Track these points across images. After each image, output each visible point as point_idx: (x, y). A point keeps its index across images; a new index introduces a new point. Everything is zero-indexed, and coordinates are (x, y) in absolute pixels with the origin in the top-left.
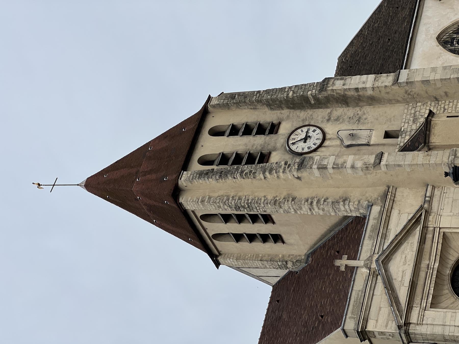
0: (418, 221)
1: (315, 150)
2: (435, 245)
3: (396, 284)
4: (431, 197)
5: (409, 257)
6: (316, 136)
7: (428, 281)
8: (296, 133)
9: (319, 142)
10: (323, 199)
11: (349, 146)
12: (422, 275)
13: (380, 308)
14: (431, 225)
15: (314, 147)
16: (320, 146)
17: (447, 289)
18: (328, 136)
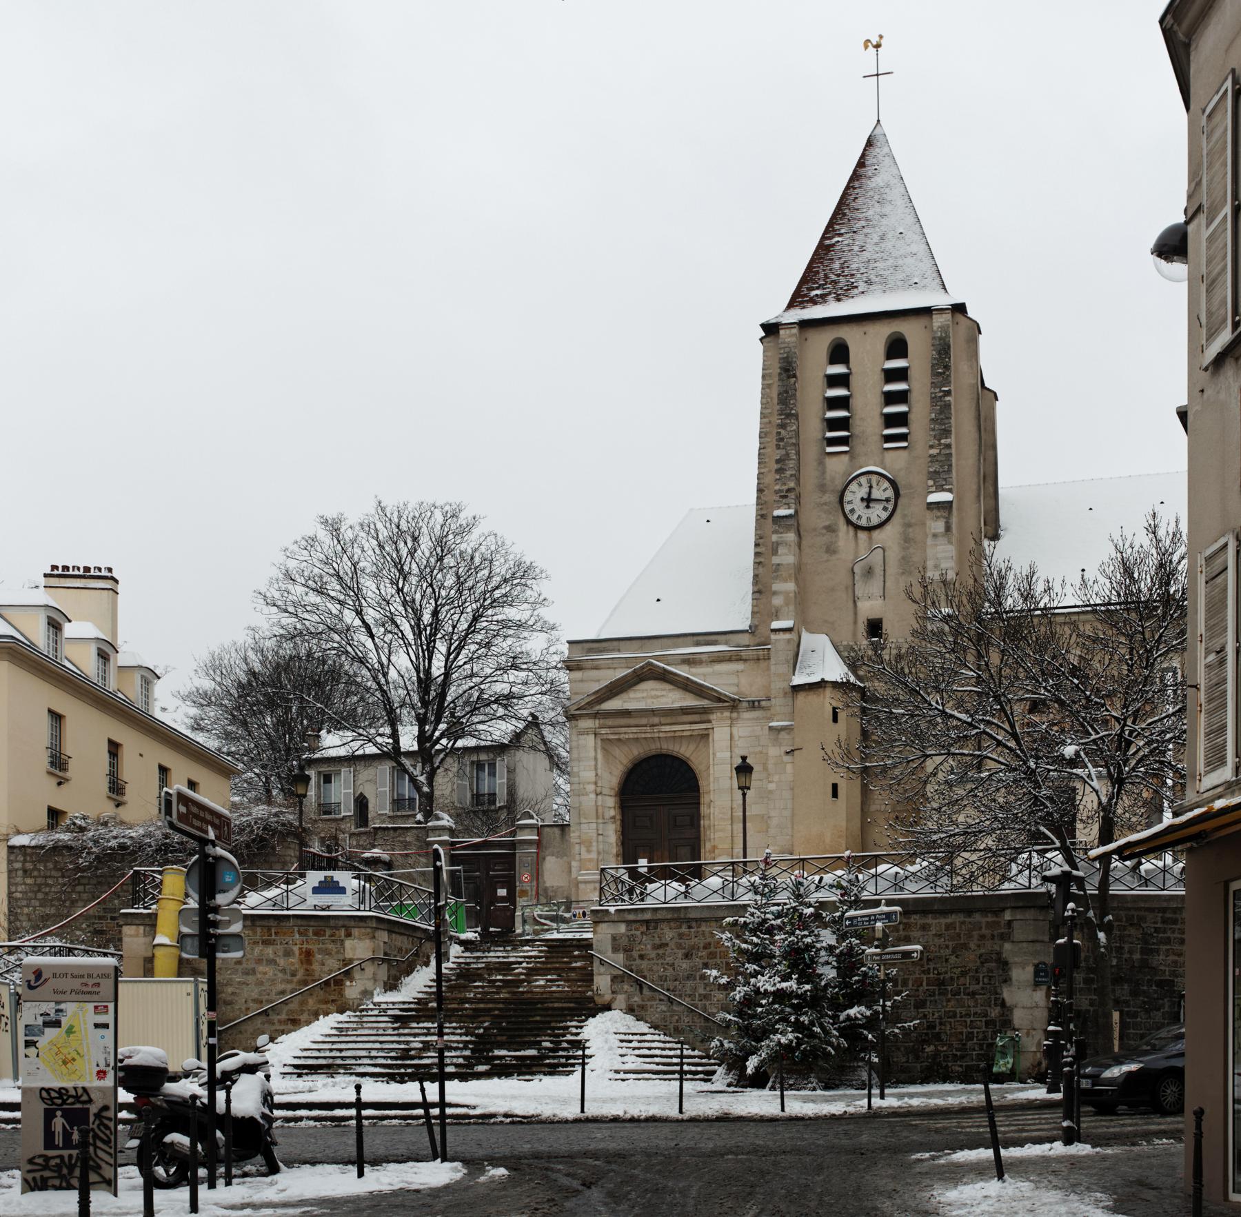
0: (720, 700)
1: (849, 522)
2: (687, 727)
3: (631, 694)
4: (760, 707)
5: (664, 700)
6: (877, 514)
7: (634, 730)
8: (882, 480)
9: (863, 523)
10: (762, 560)
11: (852, 570)
12: (644, 721)
13: (598, 681)
14: (713, 717)
15: (854, 518)
16: (857, 528)
17: (636, 752)
18: (876, 534)
